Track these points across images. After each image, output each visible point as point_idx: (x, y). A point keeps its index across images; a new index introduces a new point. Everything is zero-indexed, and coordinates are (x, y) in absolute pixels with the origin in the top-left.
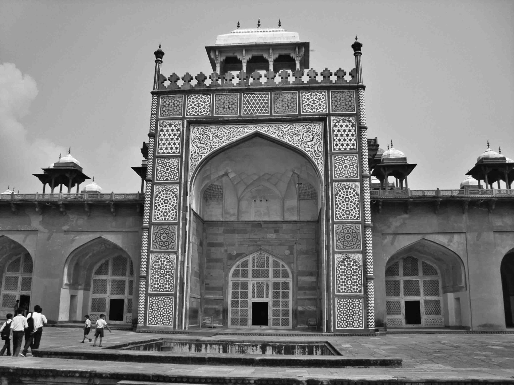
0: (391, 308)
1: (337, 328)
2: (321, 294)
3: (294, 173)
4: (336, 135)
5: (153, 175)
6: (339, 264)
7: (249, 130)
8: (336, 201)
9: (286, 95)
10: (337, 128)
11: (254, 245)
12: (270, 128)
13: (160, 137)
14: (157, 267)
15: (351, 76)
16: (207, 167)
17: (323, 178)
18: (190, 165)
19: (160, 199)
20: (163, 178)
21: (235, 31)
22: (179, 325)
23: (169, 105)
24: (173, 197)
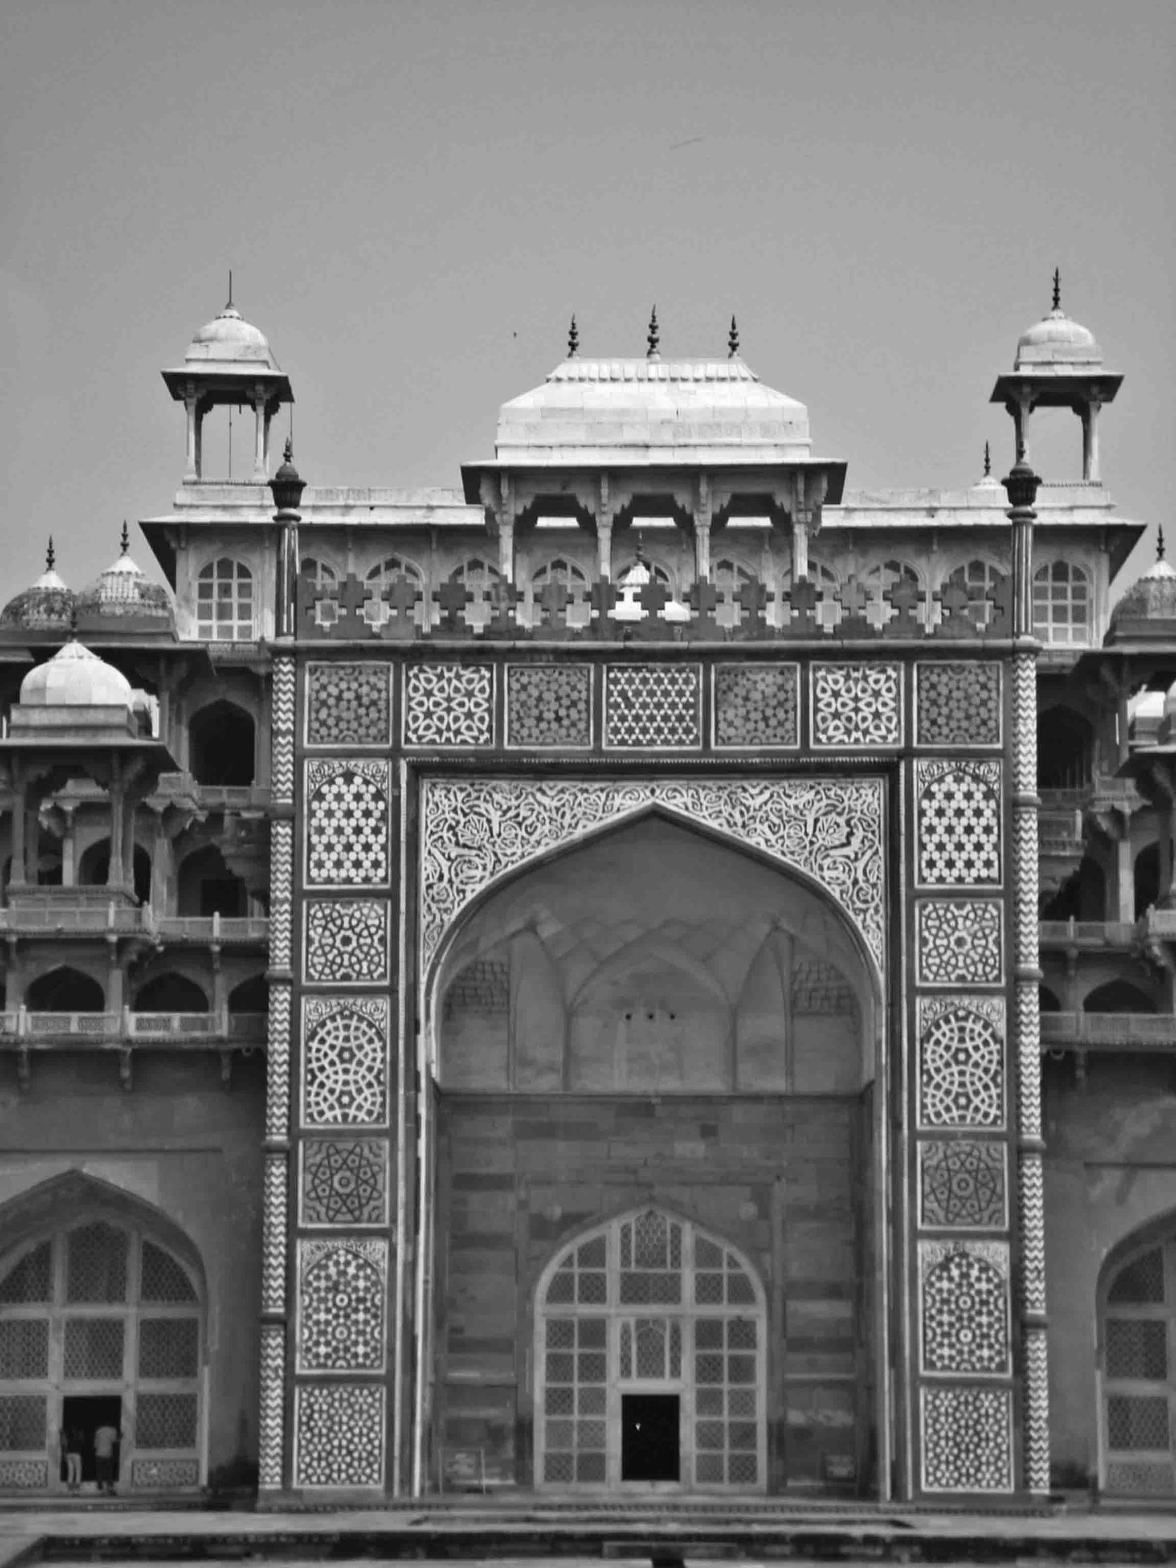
1: (924, 1488)
2: (871, 1367)
3: (776, 928)
4: (931, 830)
5: (295, 961)
6: (932, 1273)
7: (630, 800)
8: (923, 1062)
9: (758, 677)
10: (935, 804)
11: (624, 1184)
12: (702, 794)
13: (314, 822)
14: (323, 1284)
16: (476, 920)
17: (882, 977)
18: (423, 923)
19: (325, 1048)
20: (333, 973)
21: (562, 371)
22: (402, 1482)
23: (339, 698)
24: (371, 1041)
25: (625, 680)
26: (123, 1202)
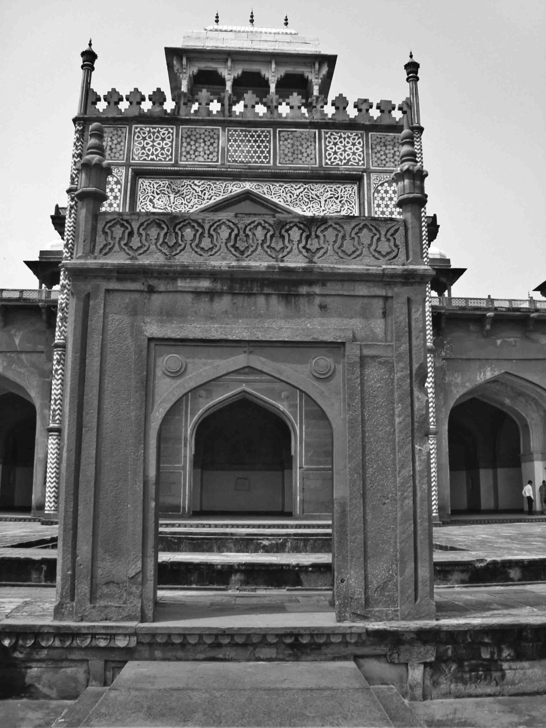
4: (379, 206)
15: (401, 112)
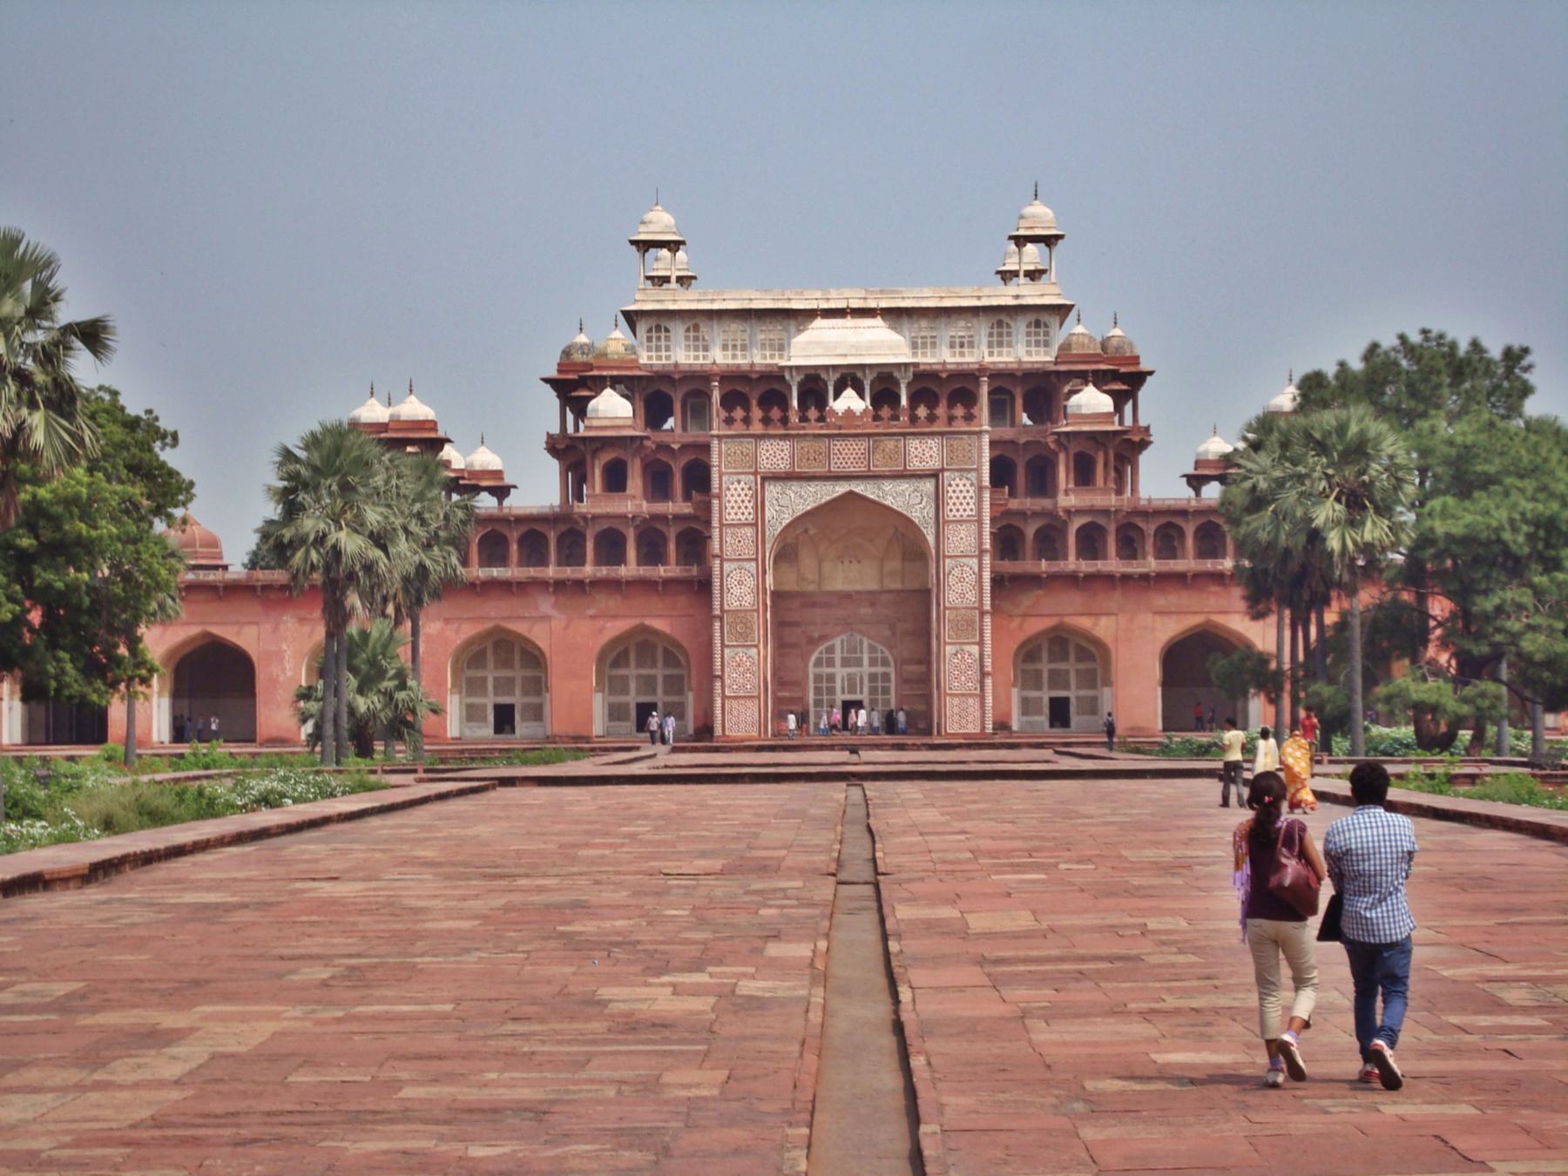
0: (1027, 707)
7: (841, 489)
25: (838, 445)
26: (656, 632)
